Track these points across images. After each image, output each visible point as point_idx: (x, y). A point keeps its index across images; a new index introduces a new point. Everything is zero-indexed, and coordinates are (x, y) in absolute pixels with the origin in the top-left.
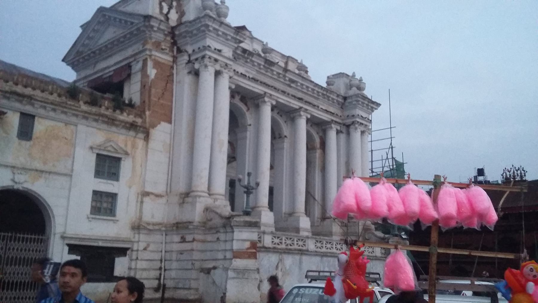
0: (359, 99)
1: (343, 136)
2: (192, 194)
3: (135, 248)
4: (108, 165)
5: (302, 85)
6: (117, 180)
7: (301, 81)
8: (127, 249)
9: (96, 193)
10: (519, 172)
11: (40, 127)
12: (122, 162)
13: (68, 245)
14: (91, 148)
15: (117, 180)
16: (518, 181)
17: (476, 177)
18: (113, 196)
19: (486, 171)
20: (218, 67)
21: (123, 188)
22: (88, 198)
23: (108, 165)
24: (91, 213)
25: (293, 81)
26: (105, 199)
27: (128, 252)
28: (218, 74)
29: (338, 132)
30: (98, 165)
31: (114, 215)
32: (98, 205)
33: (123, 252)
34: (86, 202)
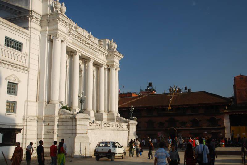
0: (116, 53)
1: (107, 72)
2: (50, 103)
3: (25, 129)
5: (92, 46)
6: (16, 95)
7: (92, 44)
8: (21, 129)
9: (8, 102)
10: (176, 89)
12: (18, 86)
15: (16, 95)
16: (176, 93)
17: (148, 87)
18: (15, 103)
19: (153, 85)
21: (19, 98)
22: (5, 104)
24: (7, 112)
25: (88, 44)
27: (22, 131)
28: (62, 41)
29: (105, 69)
31: (16, 113)
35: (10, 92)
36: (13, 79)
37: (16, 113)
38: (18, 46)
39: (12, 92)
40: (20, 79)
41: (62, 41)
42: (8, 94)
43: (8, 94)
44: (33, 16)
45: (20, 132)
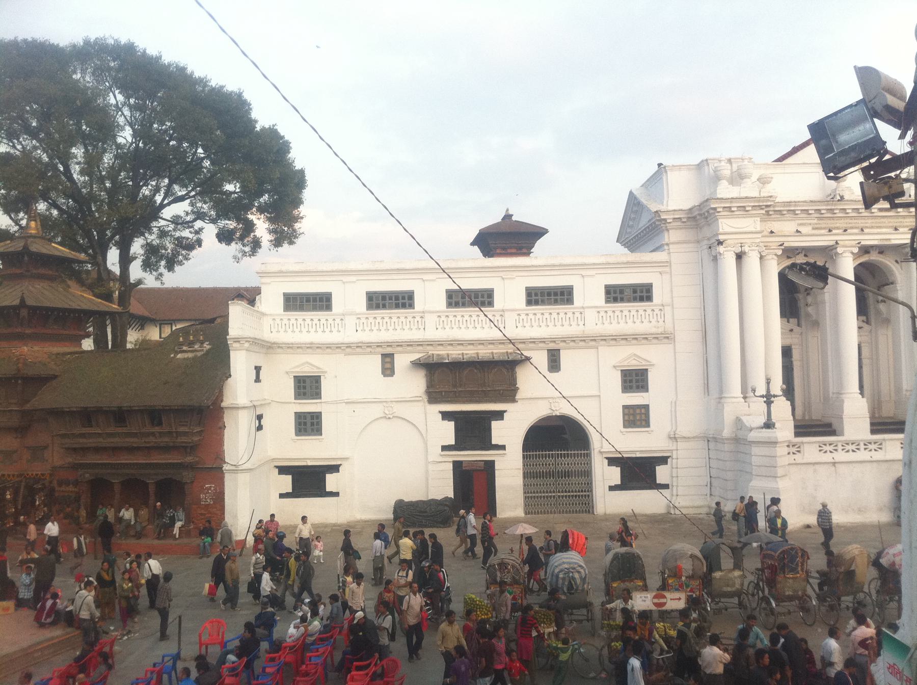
3: (674, 456)
4: (635, 379)
6: (647, 391)
8: (668, 457)
9: (625, 407)
11: (565, 357)
12: (649, 374)
13: (607, 458)
14: (614, 367)
15: (647, 391)
20: (738, 250)
21: (655, 398)
23: (635, 379)
26: (638, 411)
27: (669, 460)
30: (624, 381)
31: (649, 426)
32: (631, 418)
33: (663, 460)
34: (618, 417)
35: (631, 387)
36: (634, 362)
37: (649, 426)
38: (643, 293)
39: (638, 387)
40: (649, 359)
41: (739, 257)
42: (623, 392)
43: (623, 392)
44: (665, 220)
45: (666, 463)
